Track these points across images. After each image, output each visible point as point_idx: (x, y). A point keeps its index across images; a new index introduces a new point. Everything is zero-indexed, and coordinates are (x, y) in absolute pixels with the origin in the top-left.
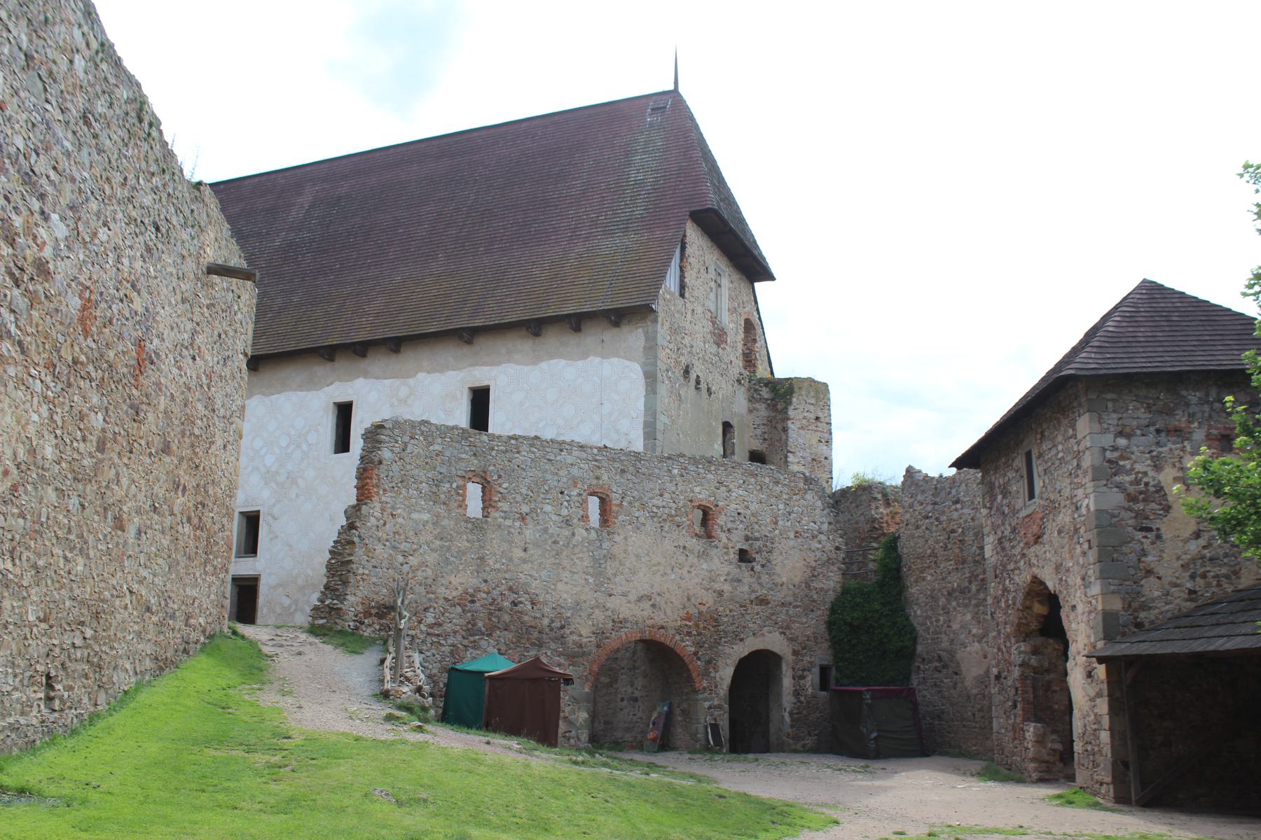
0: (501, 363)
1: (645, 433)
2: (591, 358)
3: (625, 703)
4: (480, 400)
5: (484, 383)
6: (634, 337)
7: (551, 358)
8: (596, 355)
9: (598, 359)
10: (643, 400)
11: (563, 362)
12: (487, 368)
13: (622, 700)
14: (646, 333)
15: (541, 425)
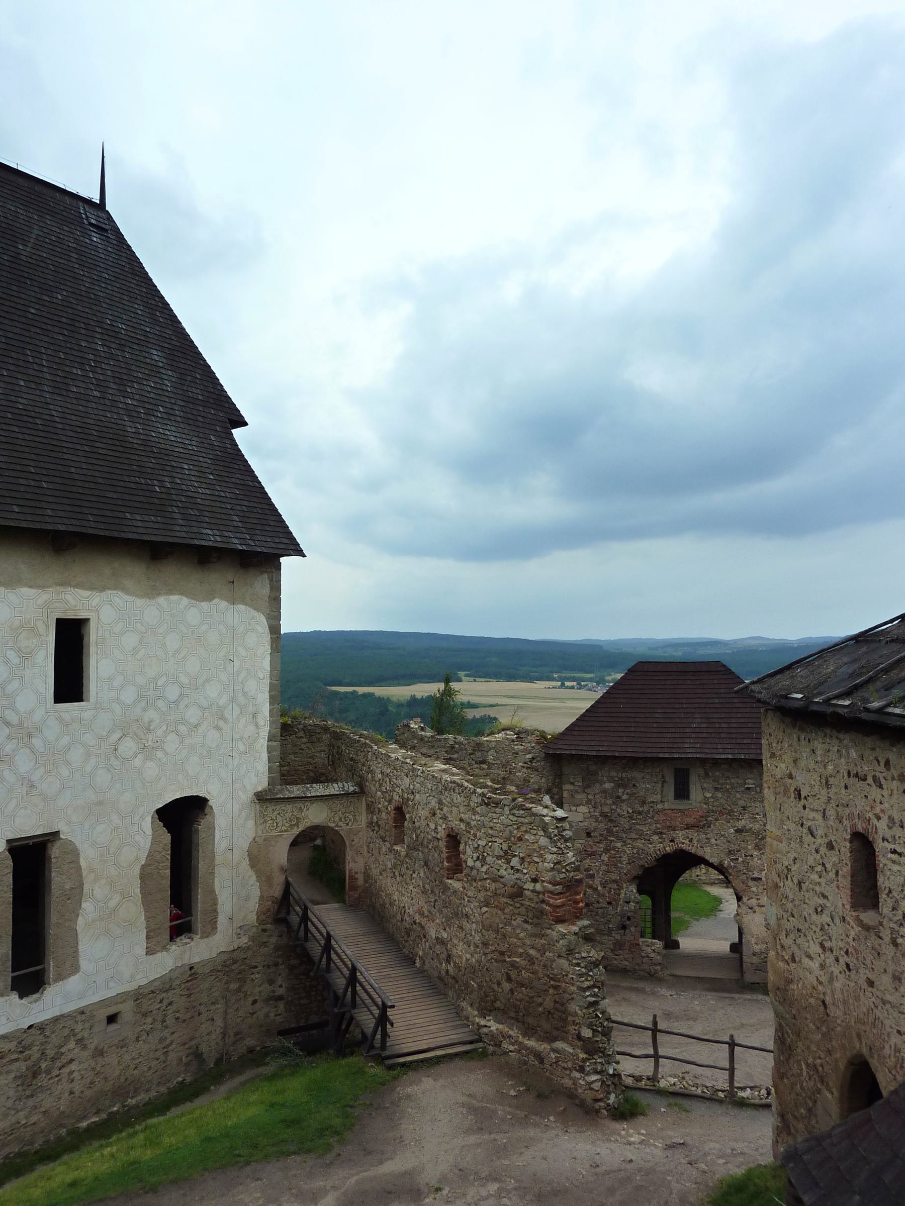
0: (103, 589)
1: (271, 697)
2: (216, 600)
3: (258, 1005)
4: (71, 638)
5: (82, 615)
6: (261, 585)
7: (170, 592)
8: (223, 597)
9: (224, 604)
10: (268, 658)
11: (185, 601)
12: (86, 593)
13: (255, 1002)
14: (271, 580)
15: (160, 683)
